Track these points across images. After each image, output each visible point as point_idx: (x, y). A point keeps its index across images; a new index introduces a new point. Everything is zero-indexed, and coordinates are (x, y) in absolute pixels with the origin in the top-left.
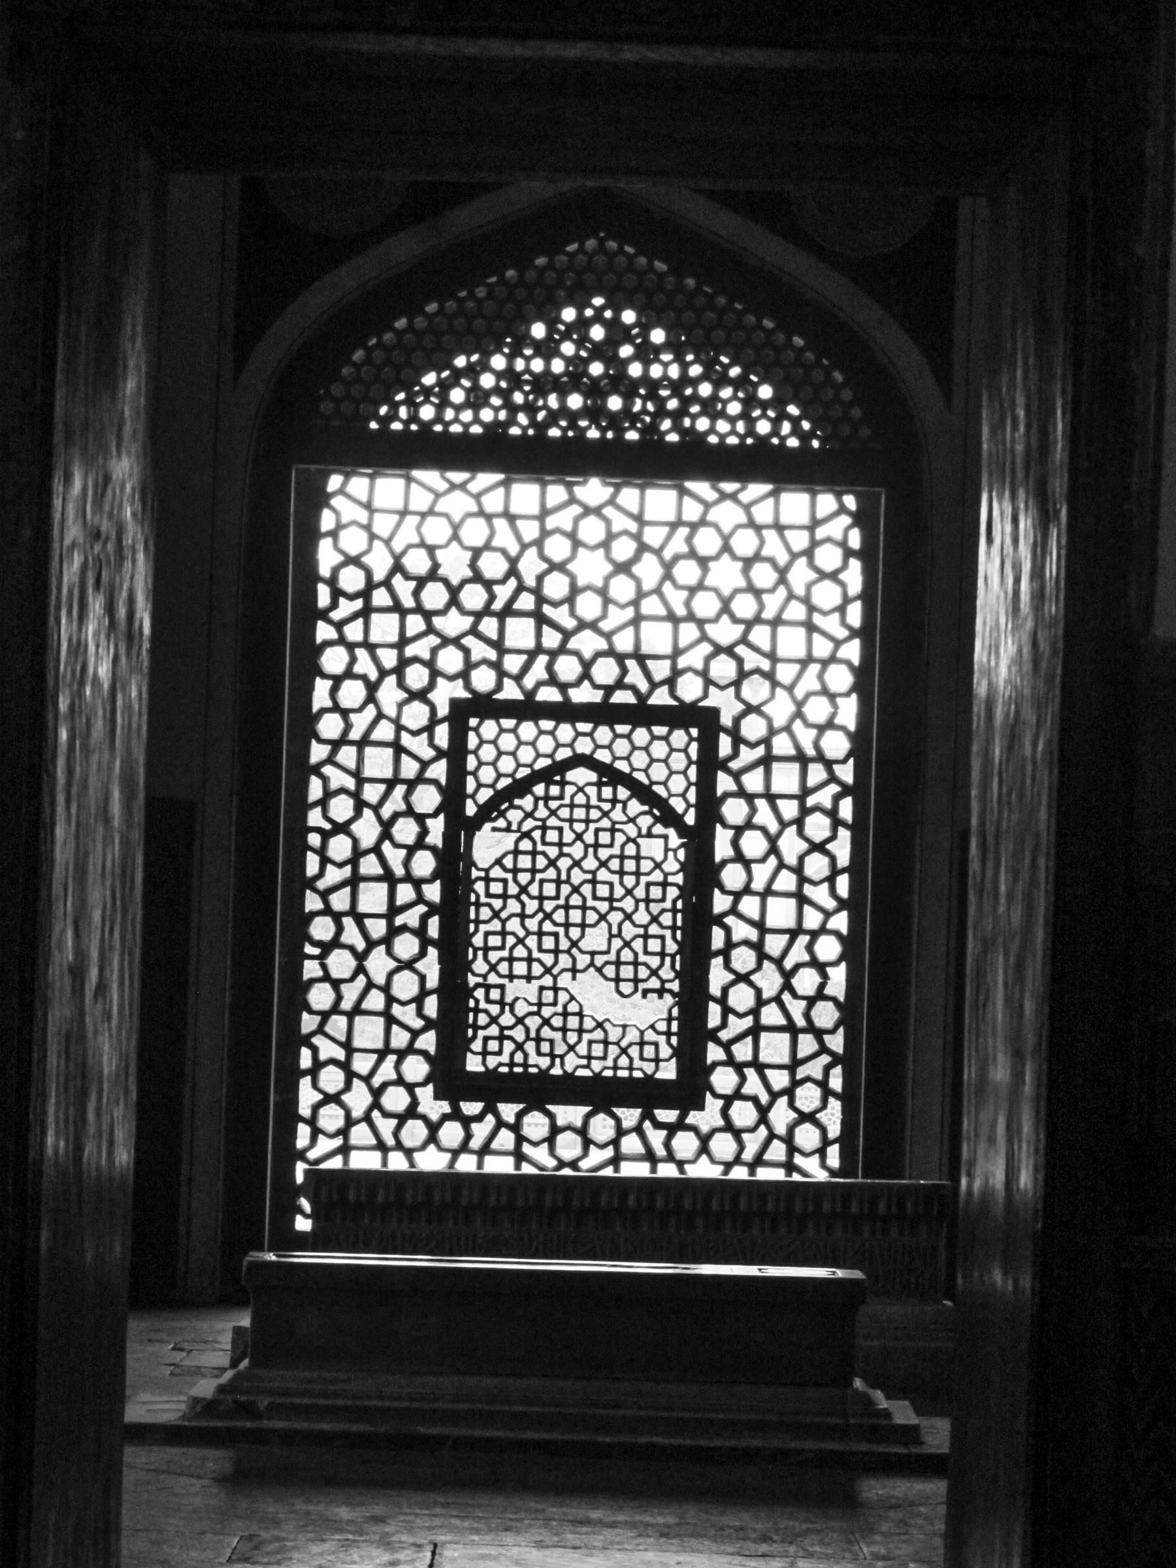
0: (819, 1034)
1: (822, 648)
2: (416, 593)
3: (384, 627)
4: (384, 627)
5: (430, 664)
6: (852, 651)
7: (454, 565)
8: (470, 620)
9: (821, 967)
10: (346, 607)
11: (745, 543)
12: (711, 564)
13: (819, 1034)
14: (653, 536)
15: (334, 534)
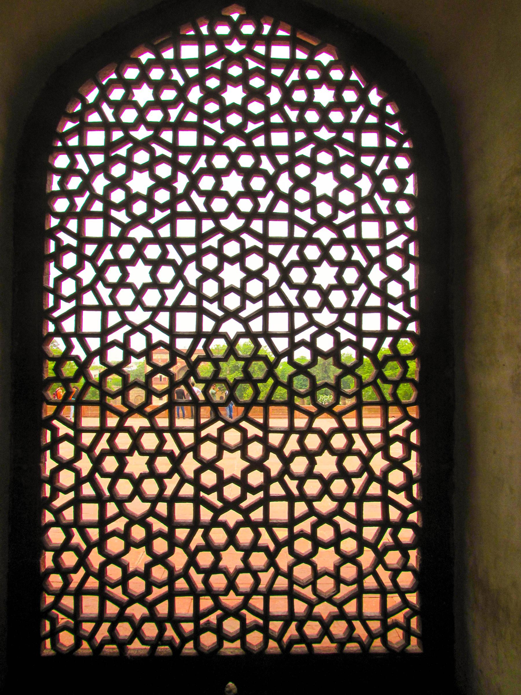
0: (402, 593)
1: (393, 325)
2: (112, 296)
3: (92, 322)
4: (92, 322)
5: (125, 346)
6: (412, 327)
7: (139, 274)
8: (150, 313)
9: (404, 549)
10: (65, 307)
11: (338, 253)
12: (316, 269)
13: (402, 593)
14: (275, 250)
15: (57, 258)
